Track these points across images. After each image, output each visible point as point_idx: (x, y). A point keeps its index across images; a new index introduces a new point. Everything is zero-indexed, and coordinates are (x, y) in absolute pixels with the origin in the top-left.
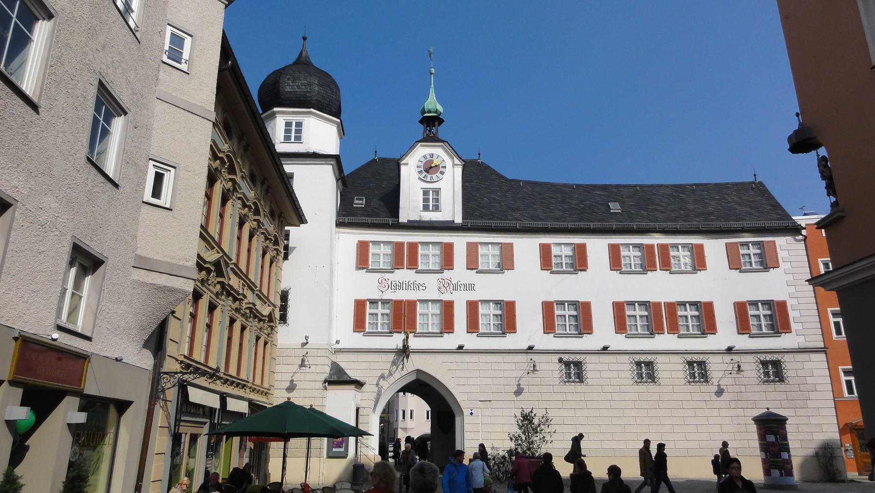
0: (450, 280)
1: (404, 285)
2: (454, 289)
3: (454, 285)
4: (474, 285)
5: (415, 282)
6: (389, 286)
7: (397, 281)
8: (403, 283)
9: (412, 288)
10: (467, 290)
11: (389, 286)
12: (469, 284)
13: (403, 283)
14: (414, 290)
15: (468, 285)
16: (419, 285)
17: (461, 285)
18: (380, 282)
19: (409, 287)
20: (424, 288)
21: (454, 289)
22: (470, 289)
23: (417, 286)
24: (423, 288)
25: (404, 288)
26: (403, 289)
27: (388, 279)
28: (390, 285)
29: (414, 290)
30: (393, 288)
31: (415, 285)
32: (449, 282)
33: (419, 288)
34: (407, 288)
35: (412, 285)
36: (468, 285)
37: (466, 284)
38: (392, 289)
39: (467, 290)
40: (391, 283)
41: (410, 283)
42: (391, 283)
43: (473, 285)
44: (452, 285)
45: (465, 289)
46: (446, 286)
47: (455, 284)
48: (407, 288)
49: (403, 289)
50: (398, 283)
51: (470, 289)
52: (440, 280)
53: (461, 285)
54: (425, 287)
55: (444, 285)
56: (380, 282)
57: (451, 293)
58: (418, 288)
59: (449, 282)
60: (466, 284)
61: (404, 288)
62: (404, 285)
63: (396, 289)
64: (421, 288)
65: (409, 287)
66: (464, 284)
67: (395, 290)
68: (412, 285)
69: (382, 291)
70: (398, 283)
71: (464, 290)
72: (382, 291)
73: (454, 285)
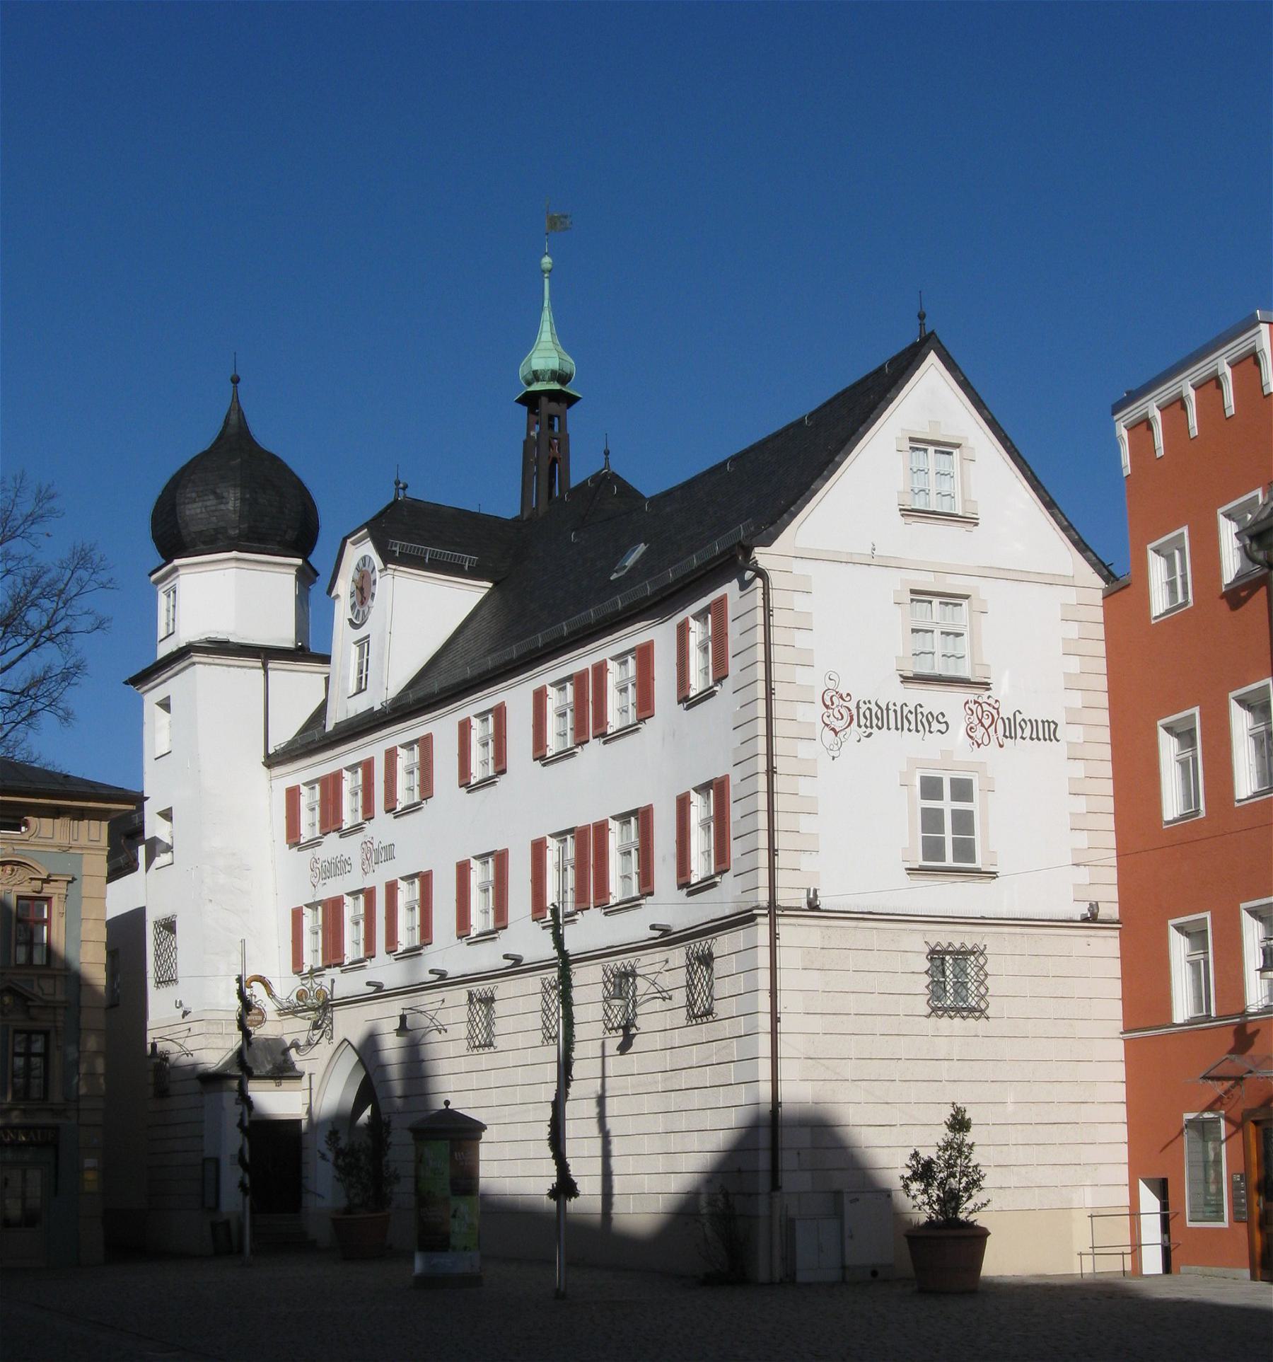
0: (996, 706)
1: (892, 714)
2: (1007, 734)
3: (1007, 722)
4: (1056, 725)
5: (919, 710)
6: (852, 720)
7: (873, 703)
8: (888, 709)
9: (913, 727)
10: (1039, 739)
11: (852, 720)
12: (1043, 722)
13: (888, 709)
14: (918, 731)
15: (1040, 725)
16: (931, 719)
17: (1023, 723)
18: (828, 703)
19: (905, 720)
20: (943, 727)
21: (1007, 734)
22: (1047, 737)
23: (924, 720)
24: (943, 727)
25: (892, 725)
26: (889, 729)
27: (848, 695)
28: (854, 712)
29: (918, 731)
30: (863, 721)
31: (920, 716)
32: (994, 712)
33: (930, 727)
34: (899, 726)
35: (912, 717)
36: (1040, 725)
37: (1036, 721)
38: (860, 726)
39: (1039, 739)
40: (858, 707)
41: (906, 710)
42: (858, 707)
43: (1052, 726)
44: (1000, 721)
45: (1034, 736)
46: (987, 722)
47: (1008, 719)
48: (899, 726)
49: (889, 729)
50: (875, 709)
51: (1047, 737)
52: (974, 707)
53: (1022, 723)
54: (946, 723)
55: (980, 721)
56: (828, 703)
57: (1001, 746)
58: (927, 729)
59: (994, 712)
60: (1036, 721)
61: (892, 725)
62: (892, 714)
63: (872, 727)
64: (935, 726)
65: (905, 720)
66: (1030, 721)
67: (869, 730)
68: (912, 717)
69: (833, 729)
70: (875, 709)
71: (1032, 739)
72: (833, 729)
73: (1007, 722)
